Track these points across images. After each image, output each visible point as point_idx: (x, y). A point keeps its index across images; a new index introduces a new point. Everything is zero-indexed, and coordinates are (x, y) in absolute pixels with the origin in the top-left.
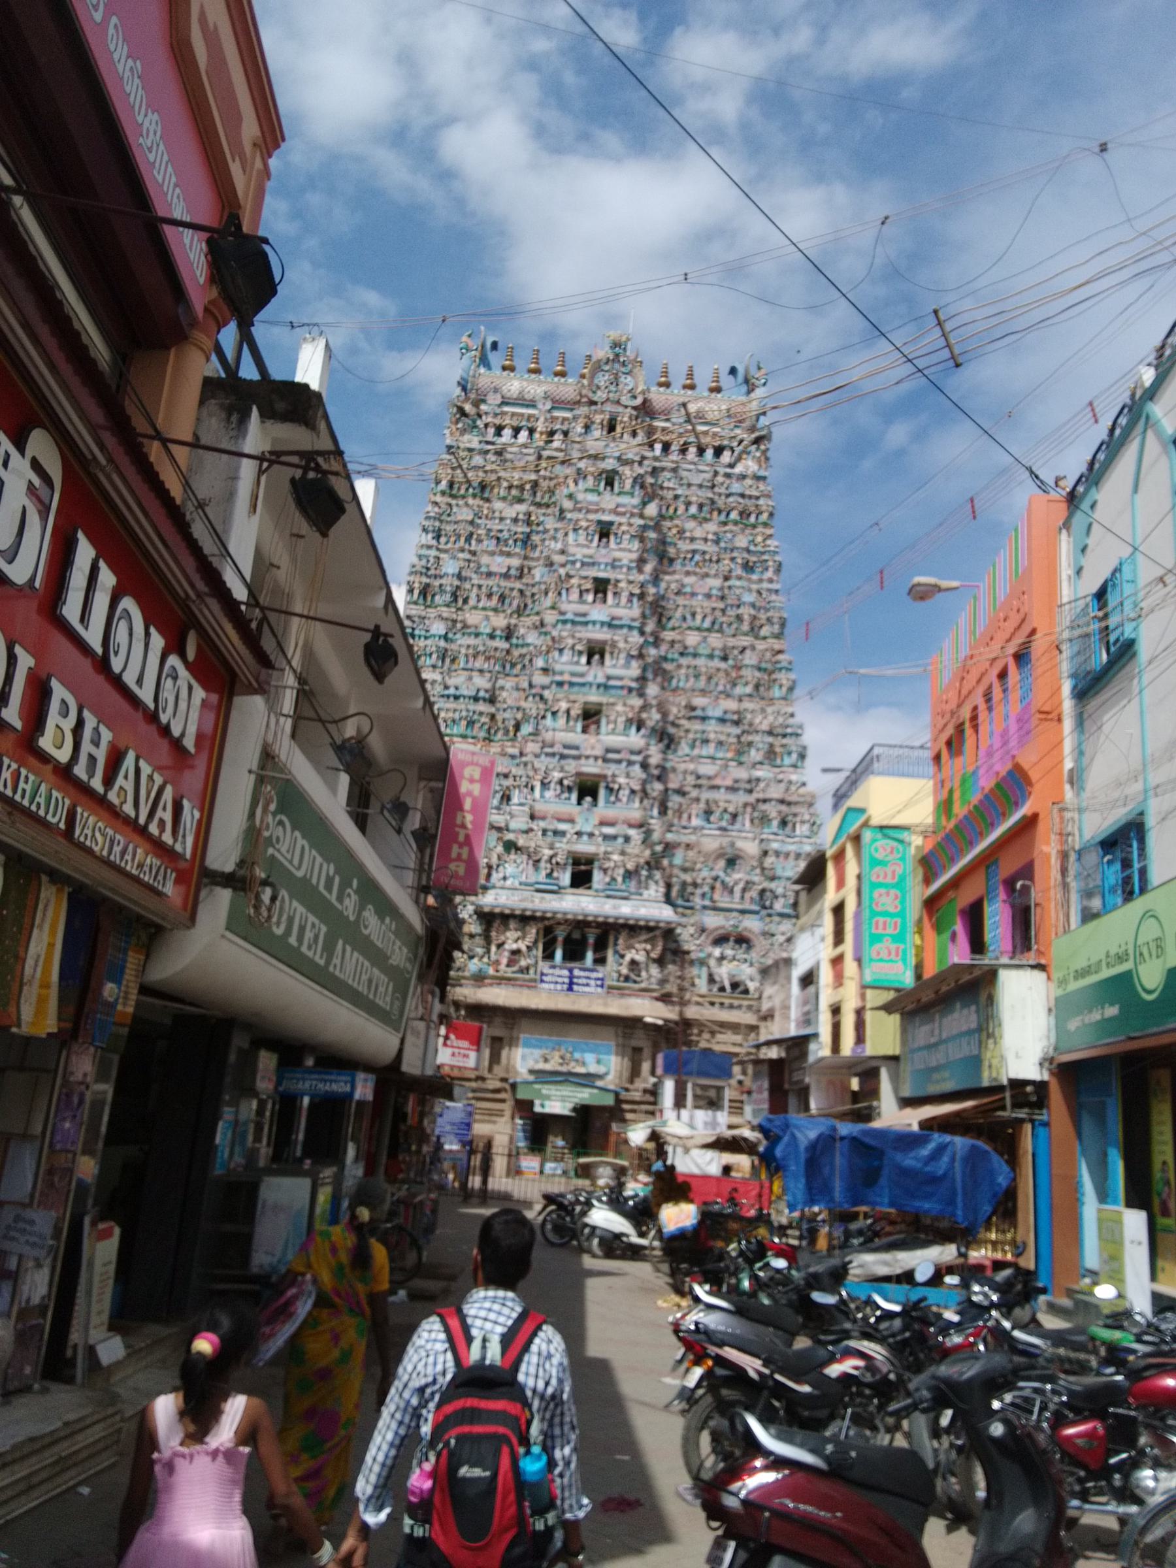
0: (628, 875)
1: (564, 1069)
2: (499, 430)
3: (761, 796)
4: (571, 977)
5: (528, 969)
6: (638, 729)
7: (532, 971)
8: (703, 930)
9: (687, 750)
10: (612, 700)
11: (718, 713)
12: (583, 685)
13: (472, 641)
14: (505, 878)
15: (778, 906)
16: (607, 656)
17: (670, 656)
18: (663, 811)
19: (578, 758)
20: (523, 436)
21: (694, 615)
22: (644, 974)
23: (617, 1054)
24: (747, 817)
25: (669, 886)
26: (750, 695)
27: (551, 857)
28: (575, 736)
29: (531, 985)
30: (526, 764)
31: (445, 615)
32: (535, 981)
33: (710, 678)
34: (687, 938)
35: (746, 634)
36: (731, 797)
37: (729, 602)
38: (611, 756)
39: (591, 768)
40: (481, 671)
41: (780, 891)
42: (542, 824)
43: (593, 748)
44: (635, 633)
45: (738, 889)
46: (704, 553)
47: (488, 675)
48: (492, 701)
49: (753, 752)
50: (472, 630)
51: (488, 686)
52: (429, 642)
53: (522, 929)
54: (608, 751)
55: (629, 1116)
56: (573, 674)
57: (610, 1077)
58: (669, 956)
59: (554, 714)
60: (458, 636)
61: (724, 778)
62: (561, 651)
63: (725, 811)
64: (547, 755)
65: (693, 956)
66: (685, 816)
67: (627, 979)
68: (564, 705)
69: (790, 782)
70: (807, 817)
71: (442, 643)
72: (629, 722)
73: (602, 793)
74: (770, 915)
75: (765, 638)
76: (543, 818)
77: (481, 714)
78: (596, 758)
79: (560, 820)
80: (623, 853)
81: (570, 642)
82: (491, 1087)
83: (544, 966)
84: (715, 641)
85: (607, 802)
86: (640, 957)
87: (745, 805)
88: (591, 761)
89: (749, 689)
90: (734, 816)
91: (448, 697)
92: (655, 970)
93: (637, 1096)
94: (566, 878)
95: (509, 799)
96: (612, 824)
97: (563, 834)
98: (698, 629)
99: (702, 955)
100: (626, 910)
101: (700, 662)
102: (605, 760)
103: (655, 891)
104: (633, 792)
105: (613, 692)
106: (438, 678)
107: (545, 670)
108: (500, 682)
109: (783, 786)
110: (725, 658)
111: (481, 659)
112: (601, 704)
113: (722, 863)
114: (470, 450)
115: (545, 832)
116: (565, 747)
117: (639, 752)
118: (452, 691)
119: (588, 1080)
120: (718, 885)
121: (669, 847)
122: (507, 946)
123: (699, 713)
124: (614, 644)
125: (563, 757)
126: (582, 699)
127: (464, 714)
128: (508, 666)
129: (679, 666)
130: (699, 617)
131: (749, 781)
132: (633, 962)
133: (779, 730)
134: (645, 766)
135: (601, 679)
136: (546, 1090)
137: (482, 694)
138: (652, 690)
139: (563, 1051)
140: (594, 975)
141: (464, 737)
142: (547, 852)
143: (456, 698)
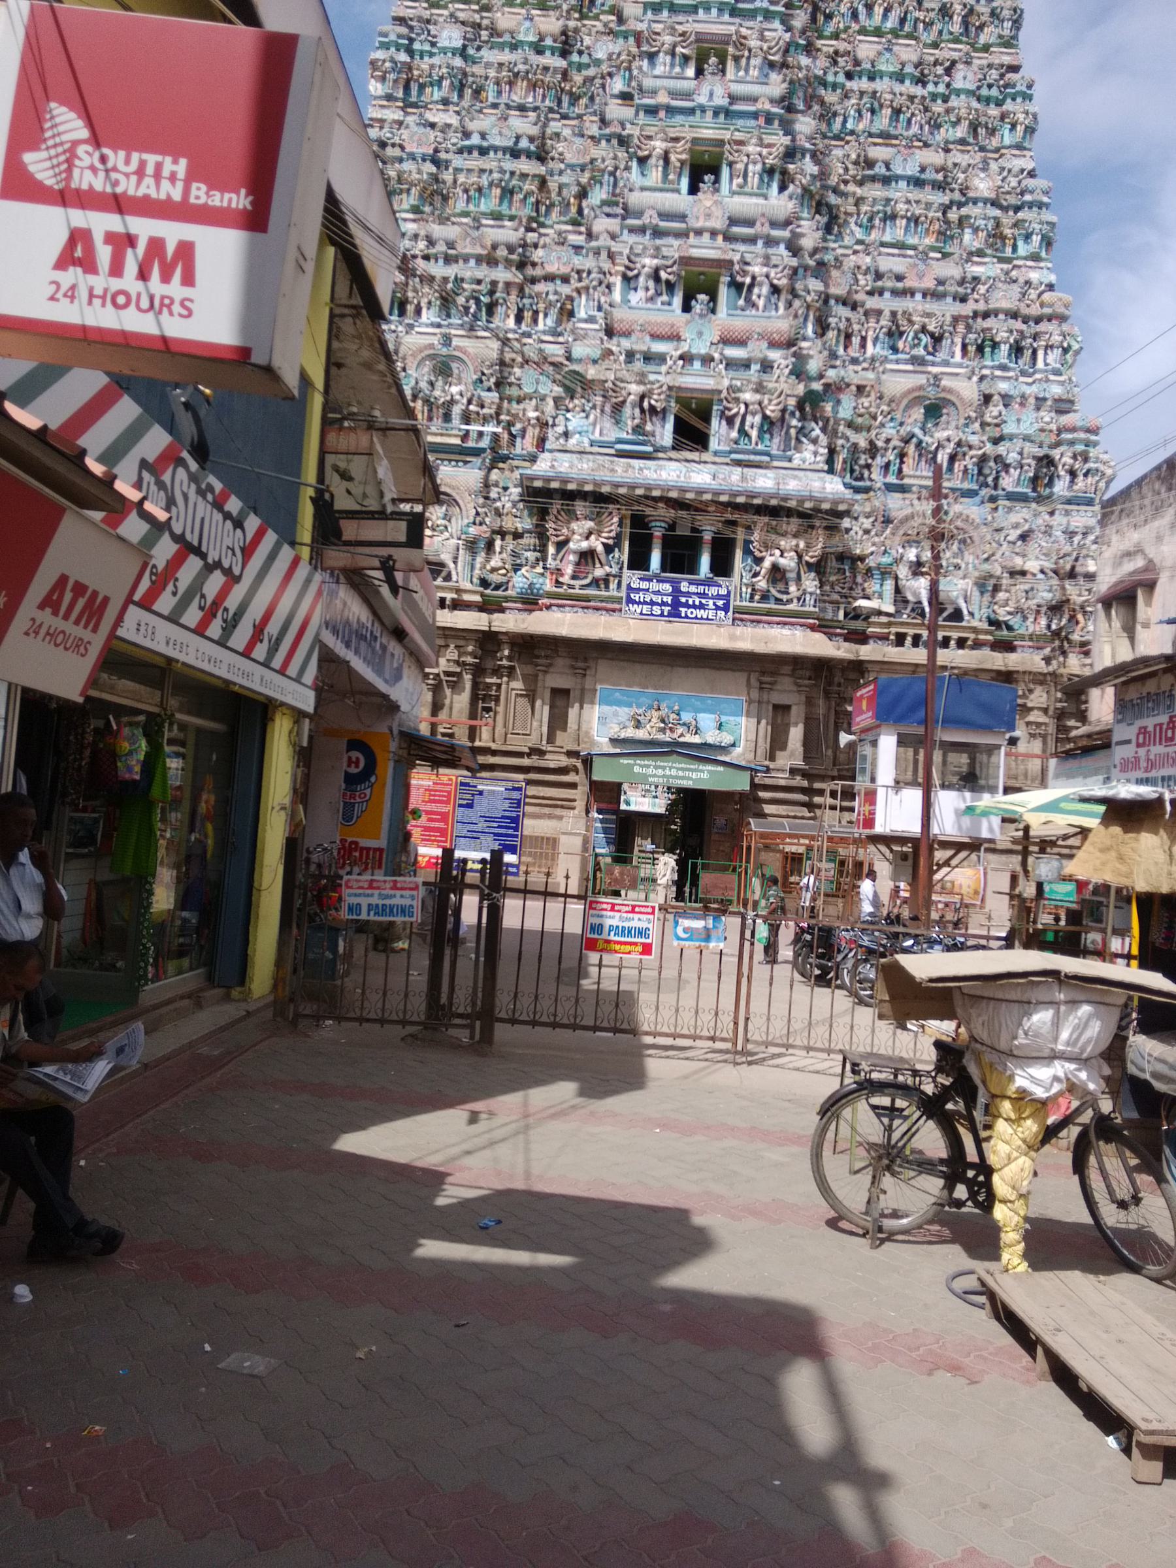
0: (769, 425)
1: (667, 737)
3: (981, 307)
4: (676, 591)
5: (606, 582)
6: (782, 188)
7: (613, 585)
8: (887, 521)
9: (859, 234)
10: (738, 136)
11: (911, 170)
12: (691, 111)
13: (506, 56)
14: (566, 434)
15: (1008, 482)
16: (730, 64)
17: (830, 78)
18: (822, 327)
19: (684, 234)
22: (793, 588)
23: (748, 715)
24: (958, 341)
25: (832, 452)
26: (962, 142)
27: (642, 397)
28: (680, 200)
29: (611, 607)
30: (597, 252)
31: (462, 16)
32: (618, 600)
33: (897, 112)
34: (859, 536)
35: (956, 41)
36: (931, 306)
38: (736, 230)
39: (705, 249)
40: (522, 108)
41: (1012, 457)
42: (626, 344)
43: (708, 216)
44: (777, 24)
45: (943, 457)
47: (532, 115)
48: (541, 156)
49: (968, 236)
50: (507, 38)
51: (534, 131)
52: (436, 60)
53: (597, 517)
54: (733, 221)
55: (769, 809)
56: (673, 94)
57: (738, 750)
58: (833, 563)
59: (642, 161)
60: (484, 52)
61: (921, 277)
62: (652, 57)
63: (924, 329)
64: (632, 230)
65: (871, 562)
66: (856, 341)
67: (765, 597)
68: (659, 145)
69: (1028, 283)
70: (1056, 338)
71: (458, 62)
72: (770, 172)
73: (723, 292)
74: (993, 499)
75: (986, 48)
76: (627, 334)
77: (524, 176)
78: (714, 233)
79: (655, 337)
80: (760, 388)
81: (668, 39)
82: (552, 765)
83: (632, 578)
84: (907, 52)
85: (733, 306)
86: (788, 562)
87: (956, 319)
88: (706, 237)
89: (961, 132)
90: (937, 339)
92: (810, 583)
93: (782, 779)
95: (571, 314)
96: (741, 343)
97: (661, 358)
99: (886, 560)
100: (764, 482)
101: (882, 85)
102: (728, 238)
103: (810, 455)
104: (775, 290)
105: (740, 122)
106: (454, 120)
107: (626, 97)
108: (555, 126)
109: (1016, 289)
110: (921, 81)
111: (522, 85)
112: (720, 143)
113: (918, 413)
115: (630, 356)
116: (663, 216)
117: (787, 223)
118: (475, 140)
119: (703, 753)
120: (911, 449)
121: (833, 390)
122: (571, 545)
123: (880, 169)
124: (741, 42)
125: (658, 233)
126: (689, 135)
127: (496, 176)
128: (565, 100)
129: (846, 96)
131: (962, 282)
132: (775, 568)
133: (1013, 200)
134: (794, 249)
135: (721, 101)
136: (639, 767)
137: (524, 144)
138: (805, 125)
139: (662, 713)
140: (713, 591)
141: (497, 216)
142: (635, 389)
143: (483, 151)
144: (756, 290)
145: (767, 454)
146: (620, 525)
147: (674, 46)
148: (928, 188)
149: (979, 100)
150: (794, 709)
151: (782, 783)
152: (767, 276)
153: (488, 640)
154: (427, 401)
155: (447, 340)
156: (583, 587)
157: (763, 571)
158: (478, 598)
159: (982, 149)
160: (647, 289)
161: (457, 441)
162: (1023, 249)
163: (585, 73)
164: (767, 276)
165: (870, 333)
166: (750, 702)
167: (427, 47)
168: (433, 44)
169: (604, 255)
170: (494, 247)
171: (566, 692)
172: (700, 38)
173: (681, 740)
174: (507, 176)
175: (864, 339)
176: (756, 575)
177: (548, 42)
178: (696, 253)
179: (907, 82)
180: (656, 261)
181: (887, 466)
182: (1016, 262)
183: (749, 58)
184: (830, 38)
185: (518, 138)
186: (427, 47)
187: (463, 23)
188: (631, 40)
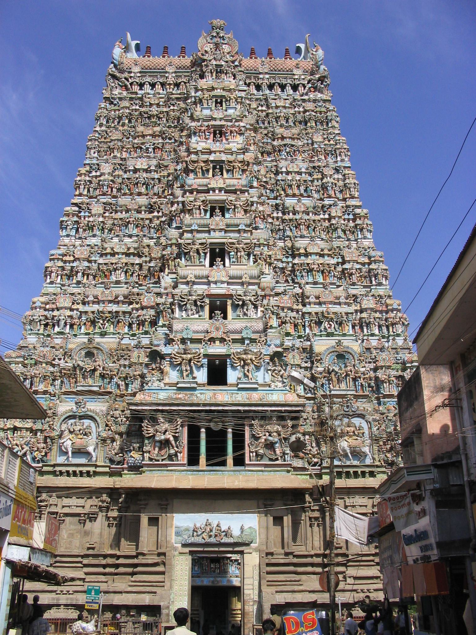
2: (141, 86)
13: (124, 215)
21: (290, 186)
37: (315, 177)
46: (293, 146)
51: (136, 245)
56: (199, 226)
73: (229, 308)
82: (150, 562)
91: (106, 254)
94: (202, 375)
98: (294, 195)
114: (121, 99)
118: (109, 250)
130: (295, 187)
137: (132, 251)
144: (246, 307)
145: (257, 383)
147: (200, 206)
148: (326, 257)
151: (282, 561)
152: (250, 301)
153: (113, 492)
158: (107, 470)
159: (348, 240)
163: (160, 219)
164: (250, 301)
167: (87, 214)
169: (170, 295)
170: (117, 297)
172: (211, 202)
173: (222, 541)
174: (124, 265)
175: (304, 326)
177: (143, 208)
178: (214, 292)
179: (311, 214)
180: (194, 297)
181: (322, 385)
182: (372, 287)
183: (235, 209)
184: (274, 199)
185: (129, 249)
186: (87, 214)
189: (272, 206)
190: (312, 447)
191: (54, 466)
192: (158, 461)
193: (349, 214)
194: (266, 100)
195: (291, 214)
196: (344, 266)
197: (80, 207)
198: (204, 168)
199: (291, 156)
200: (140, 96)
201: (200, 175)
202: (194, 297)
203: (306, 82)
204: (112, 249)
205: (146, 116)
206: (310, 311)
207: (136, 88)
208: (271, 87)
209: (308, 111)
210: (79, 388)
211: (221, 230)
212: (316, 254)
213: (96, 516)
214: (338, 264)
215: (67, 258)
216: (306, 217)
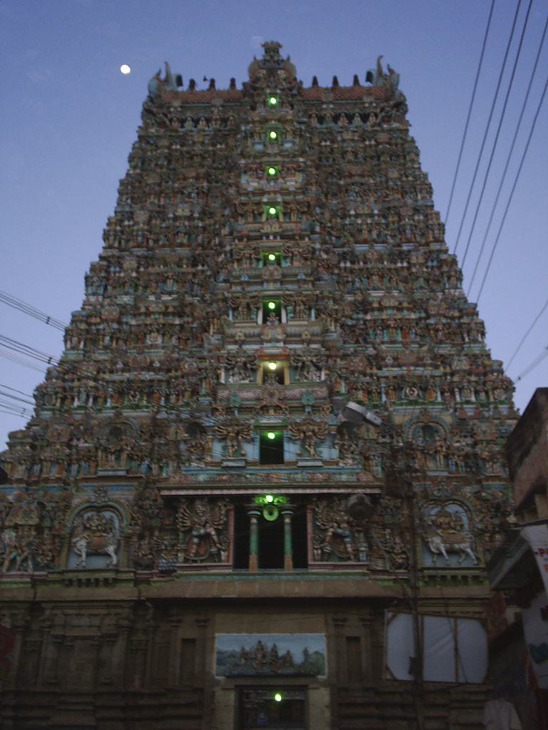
2: (182, 122)
20: (202, 124)
21: (360, 231)
26: (421, 288)
46: (362, 184)
51: (176, 304)
98: (365, 242)
114: (159, 137)
122: (195, 533)
137: (171, 310)
146: (227, 516)
149: (427, 267)
150: (363, 639)
153: (138, 604)
154: (105, 450)
155: (118, 415)
156: (202, 561)
157: (328, 539)
159: (433, 291)
160: (240, 374)
161: (122, 473)
162: (467, 340)
164: (312, 362)
165: (383, 390)
166: (328, 637)
168: (121, 268)
171: (193, 641)
173: (280, 671)
176: (323, 541)
177: (185, 261)
179: (385, 263)
180: (243, 359)
186: (118, 269)
187: (138, 257)
188: (229, 255)
189: (339, 255)
190: (395, 543)
191: (62, 573)
192: (196, 561)
193: (432, 261)
194: (331, 133)
195: (361, 263)
196: (428, 321)
197: (109, 262)
198: (256, 212)
199: (361, 197)
200: (181, 134)
201: (250, 219)
202: (243, 359)
203: (379, 110)
204: (147, 309)
205: (188, 156)
206: (387, 374)
207: (176, 125)
208: (336, 119)
209: (381, 143)
210: (101, 474)
211: (275, 281)
212: (393, 308)
213: (113, 639)
214: (420, 319)
215: (93, 320)
216: (380, 266)
